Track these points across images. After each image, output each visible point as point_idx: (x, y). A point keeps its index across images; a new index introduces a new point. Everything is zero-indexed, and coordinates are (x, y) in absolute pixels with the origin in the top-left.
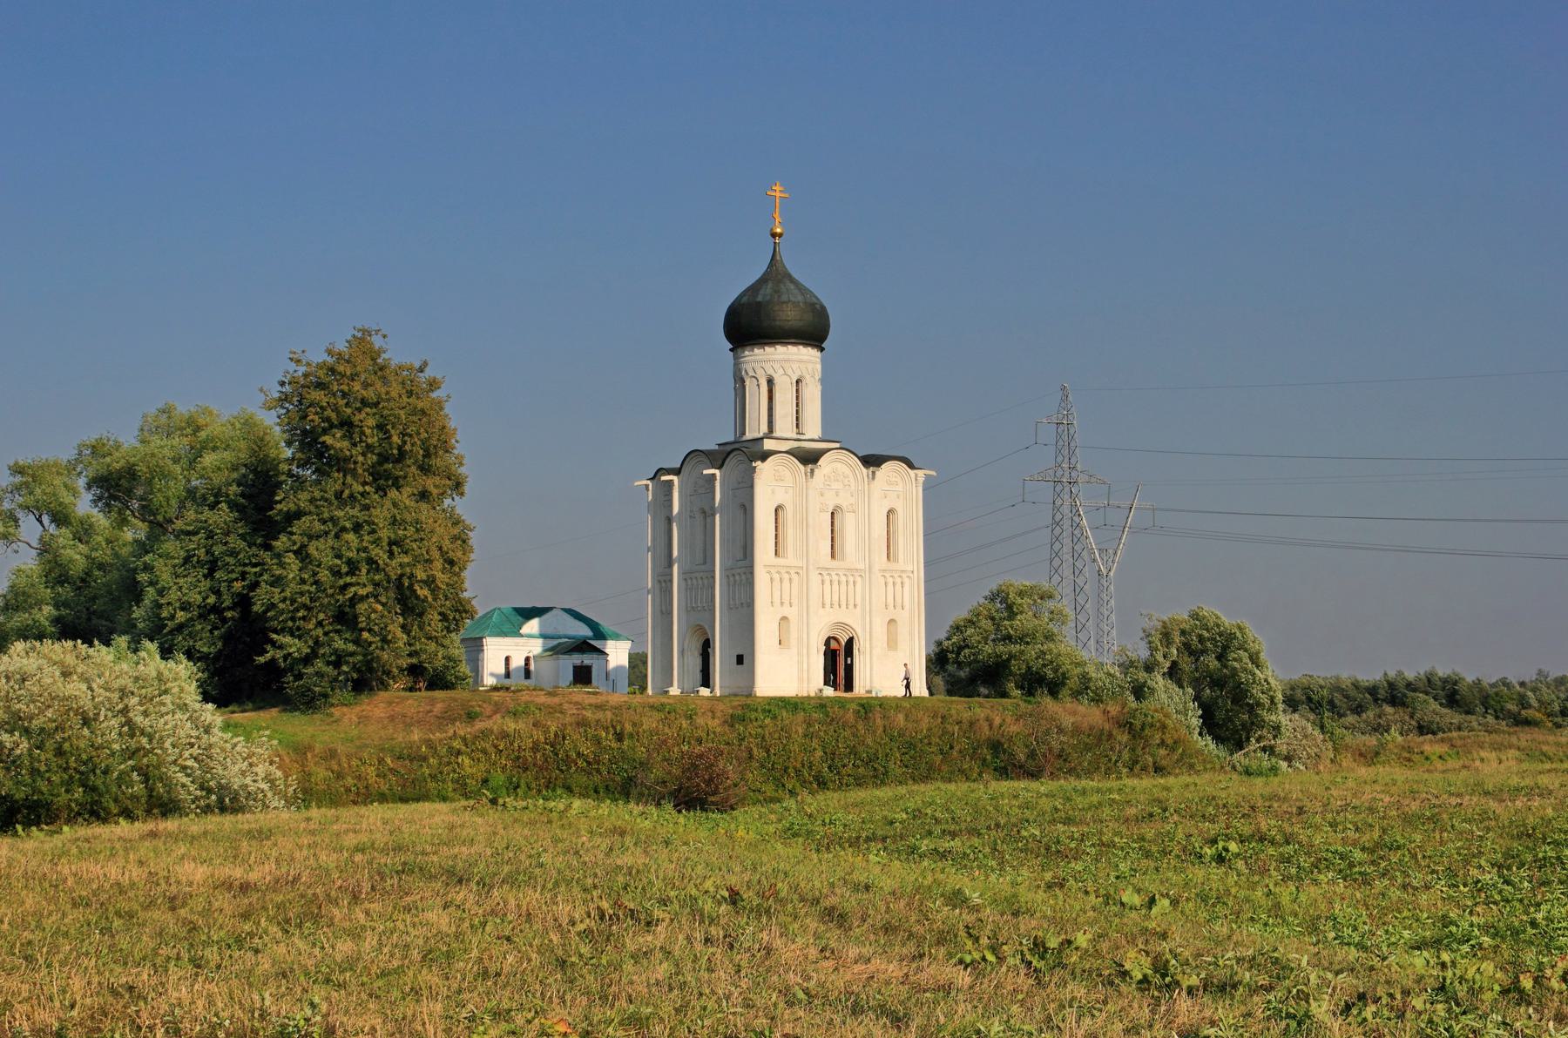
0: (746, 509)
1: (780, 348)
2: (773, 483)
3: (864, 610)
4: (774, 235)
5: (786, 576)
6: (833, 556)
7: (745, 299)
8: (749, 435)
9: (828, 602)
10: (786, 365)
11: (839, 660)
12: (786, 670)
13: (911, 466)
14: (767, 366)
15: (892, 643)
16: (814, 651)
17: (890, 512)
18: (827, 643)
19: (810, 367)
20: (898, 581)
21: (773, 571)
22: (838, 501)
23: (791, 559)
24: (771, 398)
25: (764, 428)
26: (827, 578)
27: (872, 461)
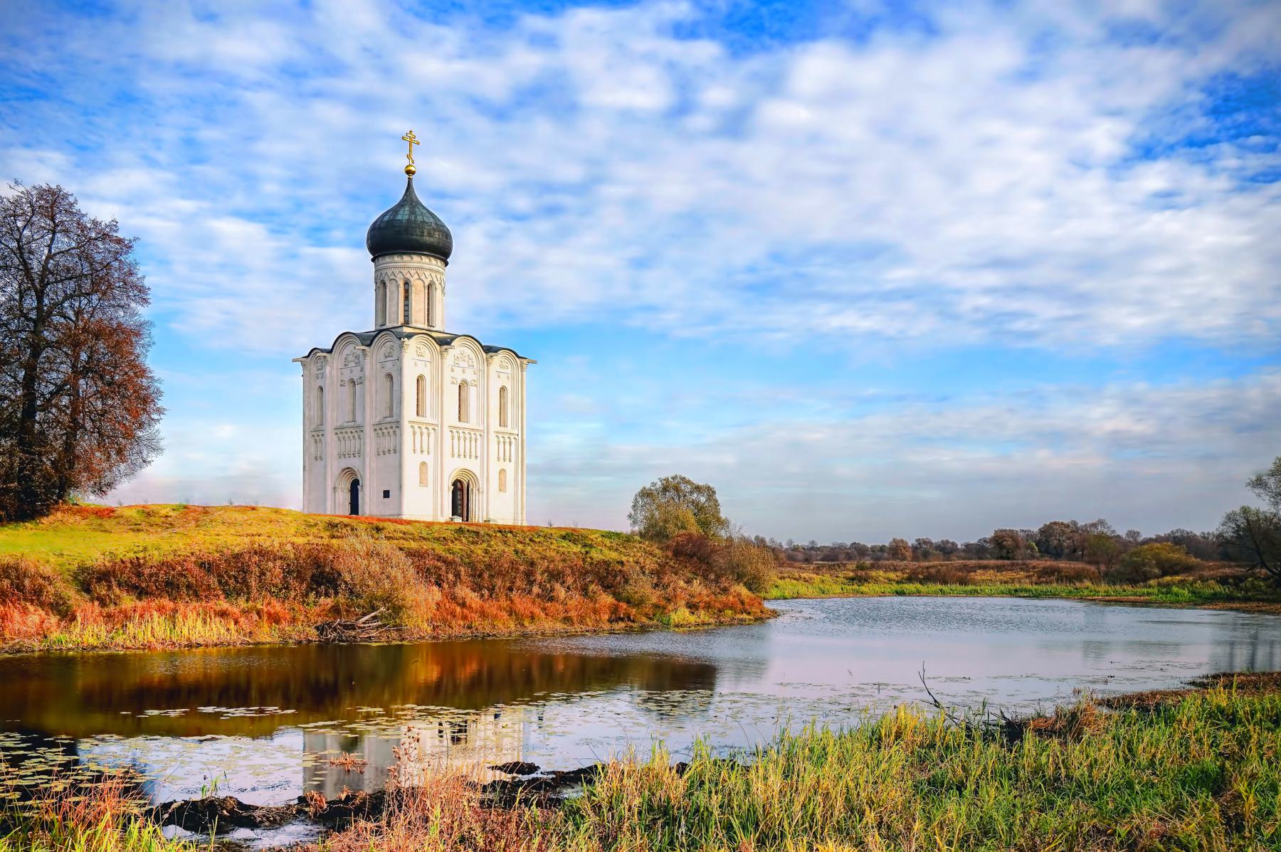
0: (393, 379)
1: (416, 258)
3: (482, 461)
5: (425, 431)
7: (386, 218)
10: (420, 272)
11: (461, 494)
12: (424, 504)
14: (405, 272)
16: (446, 488)
17: (503, 389)
18: (454, 484)
21: (416, 426)
24: (407, 298)
25: (401, 320)
26: (456, 435)
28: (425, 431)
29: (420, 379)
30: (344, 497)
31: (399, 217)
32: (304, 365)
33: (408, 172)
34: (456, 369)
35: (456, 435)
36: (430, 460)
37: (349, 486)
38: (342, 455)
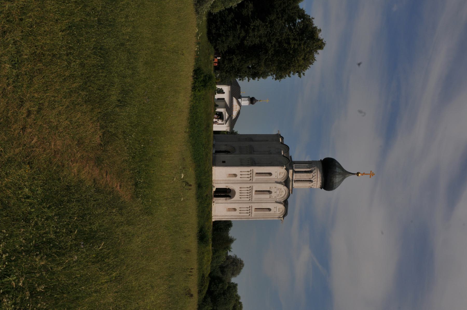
2: (278, 172)
5: (249, 176)
6: (256, 191)
7: (337, 164)
13: (284, 216)
14: (316, 171)
15: (229, 210)
17: (269, 210)
19: (316, 184)
20: (248, 212)
22: (273, 192)
23: (255, 178)
25: (296, 170)
27: (285, 203)
28: (249, 176)
29: (270, 174)
30: (223, 148)
31: (337, 168)
32: (277, 134)
33: (358, 174)
34: (276, 189)
35: (249, 189)
36: (238, 178)
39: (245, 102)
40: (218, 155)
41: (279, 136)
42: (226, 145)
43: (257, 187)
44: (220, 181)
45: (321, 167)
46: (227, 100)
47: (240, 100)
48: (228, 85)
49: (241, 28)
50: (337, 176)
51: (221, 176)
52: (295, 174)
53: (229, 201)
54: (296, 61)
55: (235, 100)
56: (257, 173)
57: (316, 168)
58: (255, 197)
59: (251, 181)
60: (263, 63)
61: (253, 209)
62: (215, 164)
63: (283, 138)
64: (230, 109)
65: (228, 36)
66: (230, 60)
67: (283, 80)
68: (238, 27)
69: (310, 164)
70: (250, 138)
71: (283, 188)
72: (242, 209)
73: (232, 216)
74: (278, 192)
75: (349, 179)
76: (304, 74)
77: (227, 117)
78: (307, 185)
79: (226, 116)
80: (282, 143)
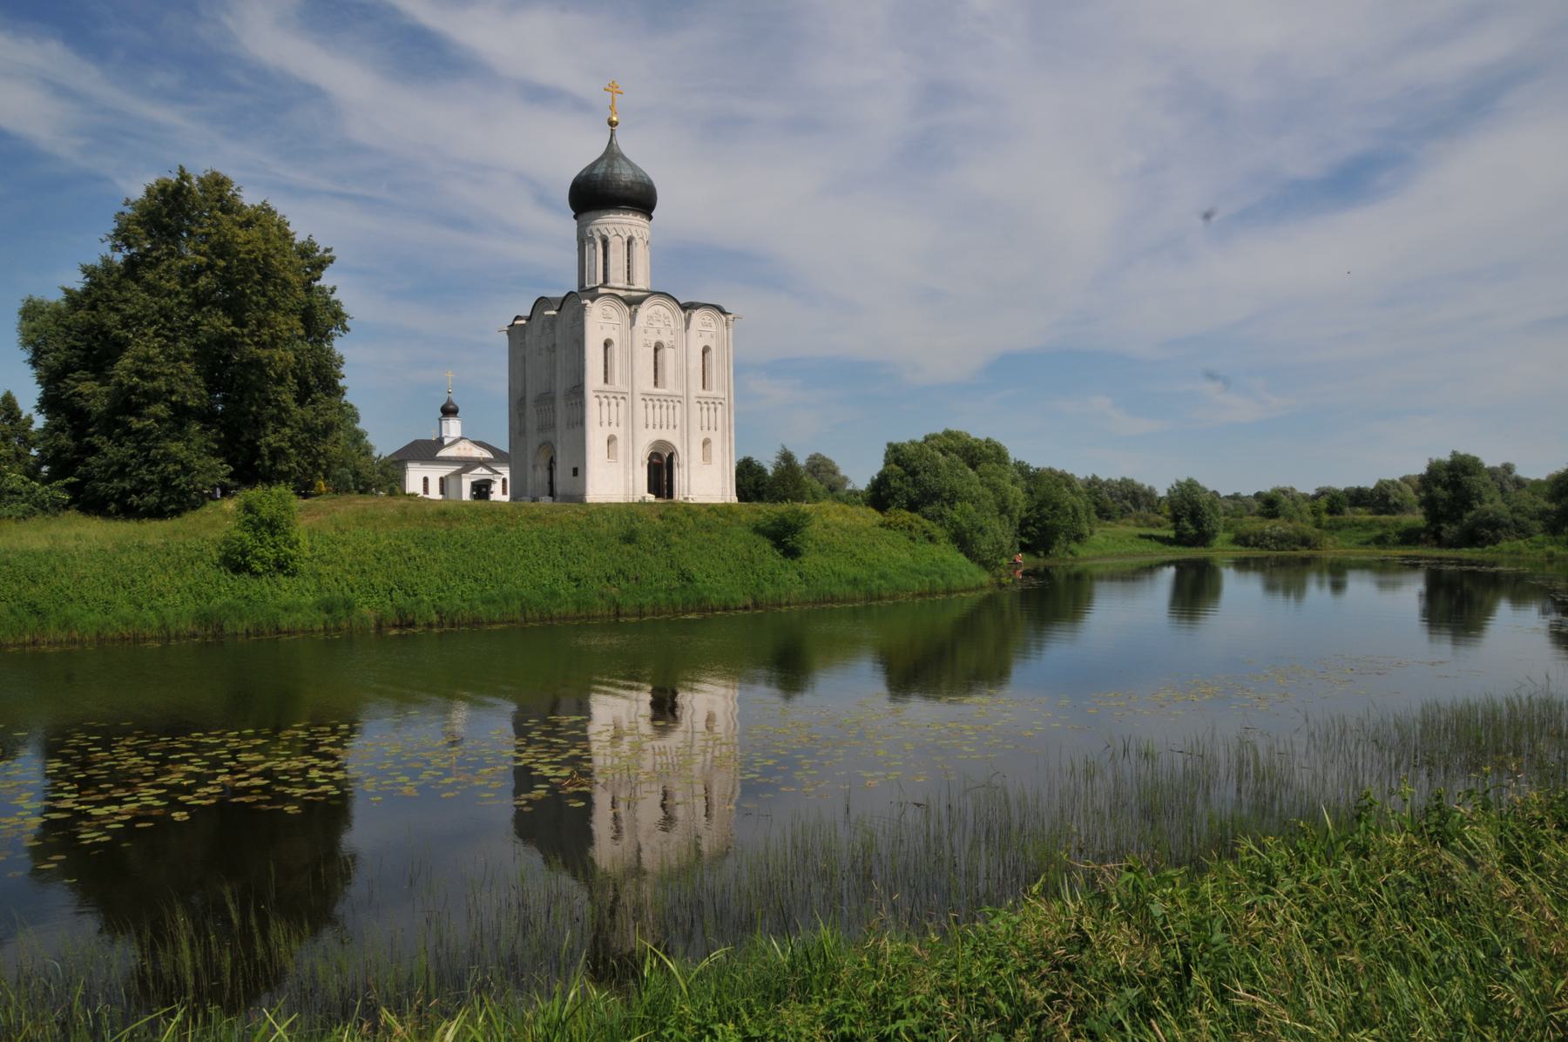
2: (600, 321)
4: (611, 123)
8: (588, 286)
9: (651, 422)
11: (661, 470)
13: (724, 313)
14: (602, 228)
15: (707, 457)
16: (638, 463)
17: (706, 350)
22: (659, 339)
23: (618, 383)
25: (600, 280)
27: (688, 307)
30: (542, 474)
36: (619, 432)
37: (547, 461)
38: (541, 429)
39: (453, 428)
40: (559, 489)
41: (513, 330)
42: (534, 467)
43: (645, 381)
44: (627, 480)
45: (593, 214)
46: (445, 471)
47: (446, 441)
48: (404, 470)
49: (139, 416)
50: (616, 171)
51: (612, 480)
52: (611, 284)
53: (681, 458)
54: (249, 246)
55: (443, 453)
56: (606, 381)
57: (594, 228)
58: (671, 386)
59: (628, 397)
60: (263, 353)
61: (705, 393)
62: (578, 498)
63: (517, 318)
64: (468, 464)
65: (167, 457)
66: (277, 454)
67: (344, 310)
68: (136, 424)
69: (583, 240)
70: (518, 405)
71: (645, 310)
72: (705, 424)
73: (723, 450)
74: (660, 325)
75: (626, 146)
76: (327, 250)
77: (485, 471)
78: (641, 254)
79: (481, 473)
80: (529, 319)
